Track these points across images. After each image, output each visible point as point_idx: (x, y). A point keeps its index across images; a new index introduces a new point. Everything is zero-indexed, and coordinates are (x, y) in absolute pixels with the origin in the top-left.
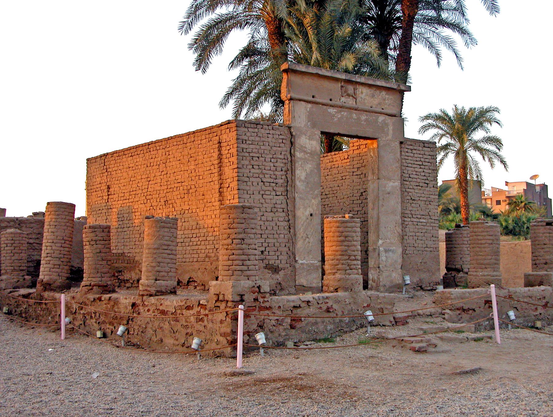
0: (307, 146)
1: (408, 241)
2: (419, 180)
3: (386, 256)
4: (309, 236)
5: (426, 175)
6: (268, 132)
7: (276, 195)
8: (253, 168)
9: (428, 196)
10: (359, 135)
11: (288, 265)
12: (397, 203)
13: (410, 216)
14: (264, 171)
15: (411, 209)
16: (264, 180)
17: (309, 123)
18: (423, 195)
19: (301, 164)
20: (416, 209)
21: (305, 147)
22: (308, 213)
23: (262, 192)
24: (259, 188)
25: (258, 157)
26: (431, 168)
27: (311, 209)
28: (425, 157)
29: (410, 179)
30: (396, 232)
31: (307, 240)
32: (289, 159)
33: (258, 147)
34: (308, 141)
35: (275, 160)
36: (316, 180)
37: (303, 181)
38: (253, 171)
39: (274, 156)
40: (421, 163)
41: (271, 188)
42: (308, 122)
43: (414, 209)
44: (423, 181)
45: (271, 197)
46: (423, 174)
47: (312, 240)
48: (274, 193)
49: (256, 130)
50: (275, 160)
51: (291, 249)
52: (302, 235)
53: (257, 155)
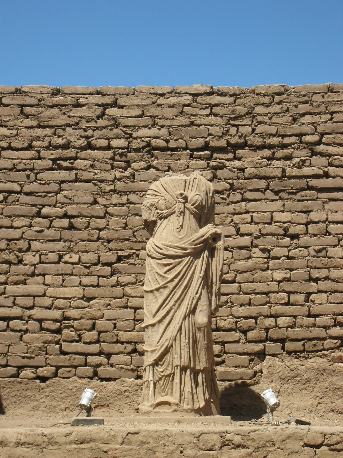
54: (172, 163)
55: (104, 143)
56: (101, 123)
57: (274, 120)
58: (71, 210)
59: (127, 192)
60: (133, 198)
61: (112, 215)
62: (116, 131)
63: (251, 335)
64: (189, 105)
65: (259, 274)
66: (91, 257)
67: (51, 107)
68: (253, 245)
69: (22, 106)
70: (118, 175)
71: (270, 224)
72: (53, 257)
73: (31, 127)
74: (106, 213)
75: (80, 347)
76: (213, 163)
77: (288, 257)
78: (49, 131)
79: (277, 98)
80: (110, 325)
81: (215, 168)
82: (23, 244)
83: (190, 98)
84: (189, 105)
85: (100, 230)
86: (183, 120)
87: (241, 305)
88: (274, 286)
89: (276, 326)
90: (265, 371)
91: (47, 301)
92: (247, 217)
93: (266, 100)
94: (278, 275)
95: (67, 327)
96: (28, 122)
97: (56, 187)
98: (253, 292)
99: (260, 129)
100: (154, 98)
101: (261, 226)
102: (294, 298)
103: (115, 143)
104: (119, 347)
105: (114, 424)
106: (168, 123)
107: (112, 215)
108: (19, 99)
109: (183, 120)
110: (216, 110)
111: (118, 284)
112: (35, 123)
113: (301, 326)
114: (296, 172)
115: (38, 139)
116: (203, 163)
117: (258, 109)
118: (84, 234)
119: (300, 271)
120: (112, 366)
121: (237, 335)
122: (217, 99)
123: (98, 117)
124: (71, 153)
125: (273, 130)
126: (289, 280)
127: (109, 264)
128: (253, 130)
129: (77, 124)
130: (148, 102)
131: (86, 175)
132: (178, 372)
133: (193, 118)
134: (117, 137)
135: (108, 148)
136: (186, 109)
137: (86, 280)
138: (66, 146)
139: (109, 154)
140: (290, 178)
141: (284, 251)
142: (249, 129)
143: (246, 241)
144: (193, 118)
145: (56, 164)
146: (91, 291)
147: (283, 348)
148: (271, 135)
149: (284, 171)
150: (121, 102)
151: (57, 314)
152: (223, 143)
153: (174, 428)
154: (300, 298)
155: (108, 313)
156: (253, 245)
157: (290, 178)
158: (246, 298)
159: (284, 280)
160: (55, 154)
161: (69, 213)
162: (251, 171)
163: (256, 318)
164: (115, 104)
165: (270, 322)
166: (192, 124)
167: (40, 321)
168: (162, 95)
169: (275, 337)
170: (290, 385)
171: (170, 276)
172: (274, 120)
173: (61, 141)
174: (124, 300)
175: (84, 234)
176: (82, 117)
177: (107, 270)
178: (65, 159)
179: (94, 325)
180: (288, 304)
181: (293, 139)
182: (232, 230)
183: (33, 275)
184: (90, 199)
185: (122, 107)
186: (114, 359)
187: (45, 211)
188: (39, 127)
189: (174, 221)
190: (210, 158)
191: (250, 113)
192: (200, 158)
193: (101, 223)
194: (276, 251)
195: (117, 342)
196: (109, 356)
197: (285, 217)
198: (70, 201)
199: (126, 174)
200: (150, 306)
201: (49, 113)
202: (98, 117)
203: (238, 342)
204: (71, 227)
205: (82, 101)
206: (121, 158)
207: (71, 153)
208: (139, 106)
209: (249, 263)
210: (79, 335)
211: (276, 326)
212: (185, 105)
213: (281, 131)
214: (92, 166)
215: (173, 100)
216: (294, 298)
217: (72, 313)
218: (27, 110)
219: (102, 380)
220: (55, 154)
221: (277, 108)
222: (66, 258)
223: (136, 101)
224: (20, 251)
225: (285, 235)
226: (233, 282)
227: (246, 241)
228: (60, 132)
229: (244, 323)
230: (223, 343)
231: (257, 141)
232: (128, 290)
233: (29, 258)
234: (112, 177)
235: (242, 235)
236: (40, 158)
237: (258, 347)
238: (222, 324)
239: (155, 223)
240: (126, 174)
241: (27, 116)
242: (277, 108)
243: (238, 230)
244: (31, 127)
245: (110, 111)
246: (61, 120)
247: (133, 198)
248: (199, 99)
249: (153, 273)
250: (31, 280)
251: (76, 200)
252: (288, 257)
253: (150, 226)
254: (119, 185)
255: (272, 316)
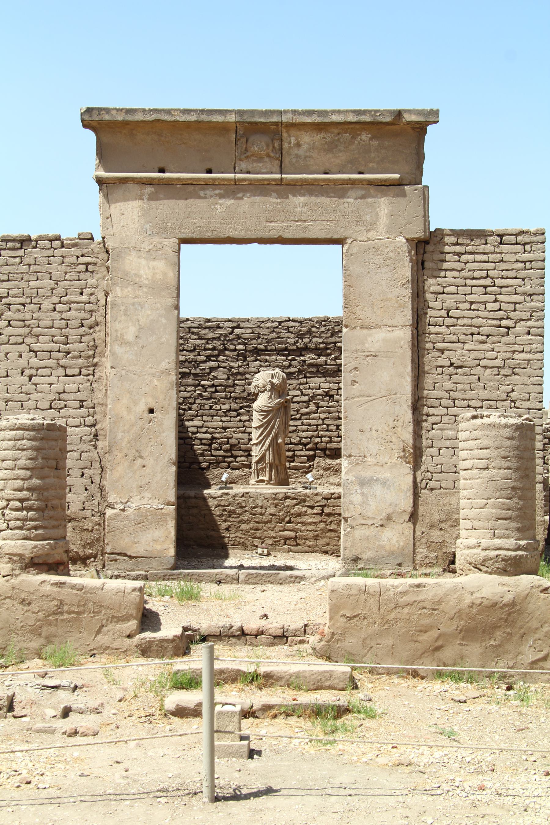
0: (142, 272)
1: (437, 460)
2: (477, 321)
3: (362, 494)
4: (145, 454)
5: (504, 306)
6: (50, 252)
7: (66, 375)
8: (9, 325)
9: (509, 355)
10: (288, 235)
11: (88, 513)
12: (401, 376)
13: (445, 402)
14: (36, 330)
15: (449, 385)
16: (35, 347)
17: (147, 226)
18: (493, 354)
19: (126, 311)
20: (467, 387)
21: (140, 276)
22: (142, 407)
23: (27, 372)
24: (23, 362)
25: (24, 305)
26: (519, 290)
27: (150, 400)
28: (503, 266)
29: (448, 321)
30: (394, 439)
31: (139, 462)
32: (103, 302)
33: (23, 284)
34: (143, 262)
35: (66, 307)
36: (163, 340)
37: (128, 343)
38: (10, 330)
39: (65, 299)
40: (488, 282)
41: (51, 363)
42: (148, 222)
43: (460, 386)
44: (497, 322)
45: (53, 379)
46: (496, 306)
47: (150, 462)
48: (61, 371)
49: (21, 253)
50: (66, 307)
51: (97, 479)
52: (125, 451)
53: (22, 300)
54: (268, 358)
55: (232, 347)
56: (231, 337)
57: (322, 335)
58: (216, 382)
59: (245, 373)
60: (248, 376)
61: (238, 385)
62: (239, 341)
63: (308, 446)
64: (277, 327)
65: (313, 415)
66: (227, 407)
67: (205, 328)
68: (309, 401)
69: (190, 328)
70: (240, 364)
71: (319, 389)
72: (207, 407)
73: (195, 339)
74: (234, 384)
75: (221, 453)
76: (289, 358)
77: (327, 407)
78: (204, 341)
79: (323, 323)
80: (236, 442)
81: (291, 360)
82: (191, 400)
83: (277, 323)
84: (277, 327)
85: (231, 393)
86: (274, 335)
87: (303, 431)
88: (320, 422)
89: (321, 442)
90: (315, 466)
91: (204, 430)
92: (307, 386)
93: (317, 325)
94: (323, 416)
95: (215, 443)
96: (193, 336)
97: (207, 371)
98: (310, 425)
99: (314, 340)
100: (259, 324)
101: (314, 391)
102: (330, 427)
103: (238, 347)
104: (241, 453)
105: (238, 489)
106: (266, 337)
107: (238, 385)
108: (188, 324)
109: (274, 335)
110: (291, 330)
111: (240, 421)
112: (196, 337)
113: (334, 442)
114: (333, 362)
115: (198, 346)
116: (284, 358)
117: (314, 329)
118: (223, 395)
119: (334, 414)
120: (237, 462)
121: (301, 447)
122: (291, 324)
123: (230, 334)
124: (215, 353)
125: (321, 340)
126: (328, 418)
127: (235, 410)
128: (311, 340)
129: (219, 337)
130: (256, 325)
131: (224, 365)
132: (268, 466)
133: (279, 334)
134: (239, 344)
135: (235, 350)
136: (275, 330)
137: (224, 419)
138: (214, 349)
139: (235, 353)
140: (330, 365)
141: (325, 403)
142: (308, 340)
143: (306, 398)
144: (279, 334)
145: (208, 358)
146: (225, 424)
147: (325, 453)
148: (320, 343)
149: (326, 361)
150: (242, 325)
151: (209, 436)
152: (295, 347)
153: (265, 491)
154: (334, 428)
155: (235, 436)
156: (309, 401)
157: (330, 365)
158: (305, 428)
159: (326, 418)
160: (207, 353)
161: (215, 384)
162: (309, 362)
163: (311, 438)
164: (238, 327)
165: (318, 440)
166: (279, 337)
167: (201, 439)
168: (263, 322)
169: (321, 447)
170: (328, 472)
171: (265, 421)
172: (322, 335)
173: (210, 346)
174: (244, 429)
175: (223, 395)
176: (221, 334)
177: (235, 413)
178: (213, 356)
179: (228, 441)
180: (327, 430)
181: (332, 345)
182: (299, 392)
183: (197, 416)
184: (226, 377)
185: (242, 328)
186: (238, 459)
187: (202, 383)
188: (199, 339)
189: (267, 394)
190: (289, 355)
191: (310, 330)
192: (283, 355)
193: (232, 389)
194: (322, 403)
195: (240, 450)
196: (235, 457)
197: (327, 385)
198: (215, 378)
199: (245, 363)
200: (255, 434)
201: (203, 332)
202: (230, 334)
203: (302, 450)
204: (216, 391)
205: (221, 325)
206: (242, 356)
207: (215, 353)
208: (250, 328)
209: (308, 410)
210: (221, 447)
211: (321, 442)
212: (275, 328)
213: (325, 341)
214: (227, 360)
215: (269, 324)
216: (330, 427)
217: (216, 435)
218: (192, 330)
219: (233, 469)
220: (207, 353)
221: (323, 329)
222: (214, 407)
223: (249, 326)
224: (190, 404)
225: (326, 396)
226: (300, 419)
227: (306, 398)
228: (210, 342)
229: (304, 441)
230: (294, 451)
231: (312, 346)
232: (246, 424)
233: (194, 407)
234: (237, 365)
235: (305, 395)
236: (199, 355)
237: (312, 453)
238: (293, 441)
239: (258, 394)
240: (245, 363)
241: (193, 333)
242: (323, 329)
243: (302, 392)
244: (195, 339)
245: (236, 331)
246: (210, 335)
247: (248, 376)
248: (282, 324)
249: (257, 420)
250: (196, 419)
251: (219, 377)
252: (327, 407)
253: (256, 395)
254: (241, 370)
255: (319, 437)
